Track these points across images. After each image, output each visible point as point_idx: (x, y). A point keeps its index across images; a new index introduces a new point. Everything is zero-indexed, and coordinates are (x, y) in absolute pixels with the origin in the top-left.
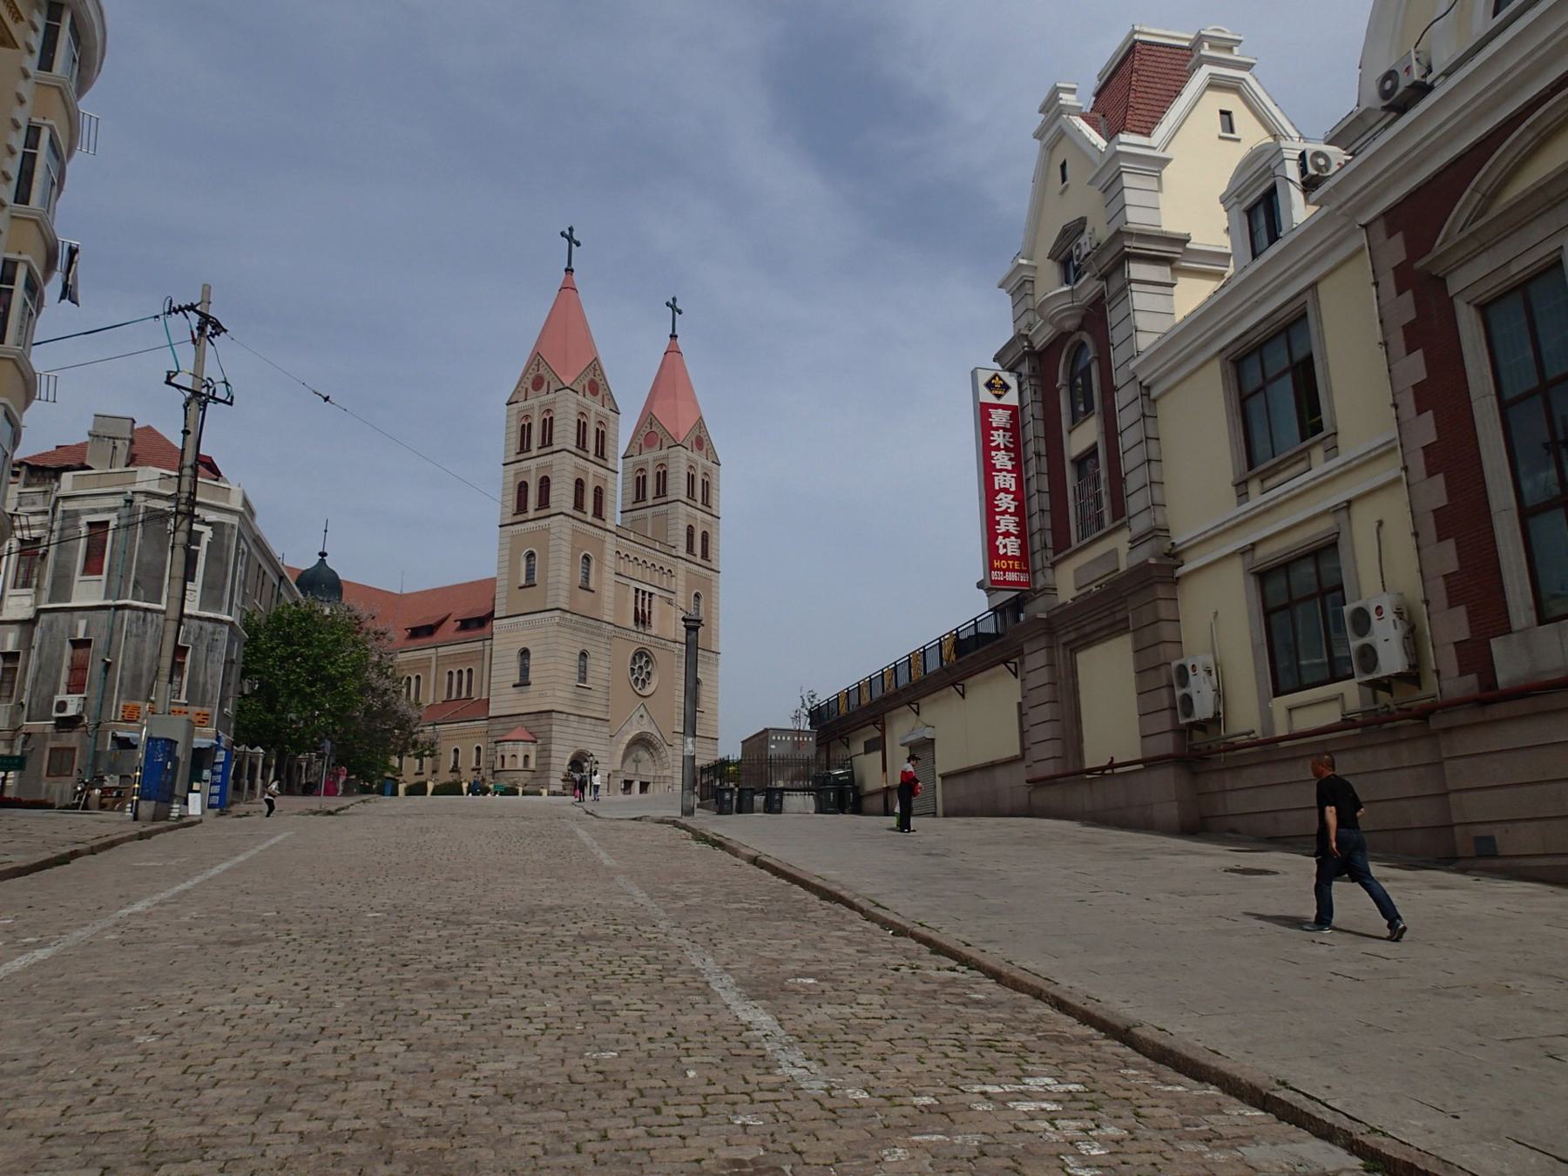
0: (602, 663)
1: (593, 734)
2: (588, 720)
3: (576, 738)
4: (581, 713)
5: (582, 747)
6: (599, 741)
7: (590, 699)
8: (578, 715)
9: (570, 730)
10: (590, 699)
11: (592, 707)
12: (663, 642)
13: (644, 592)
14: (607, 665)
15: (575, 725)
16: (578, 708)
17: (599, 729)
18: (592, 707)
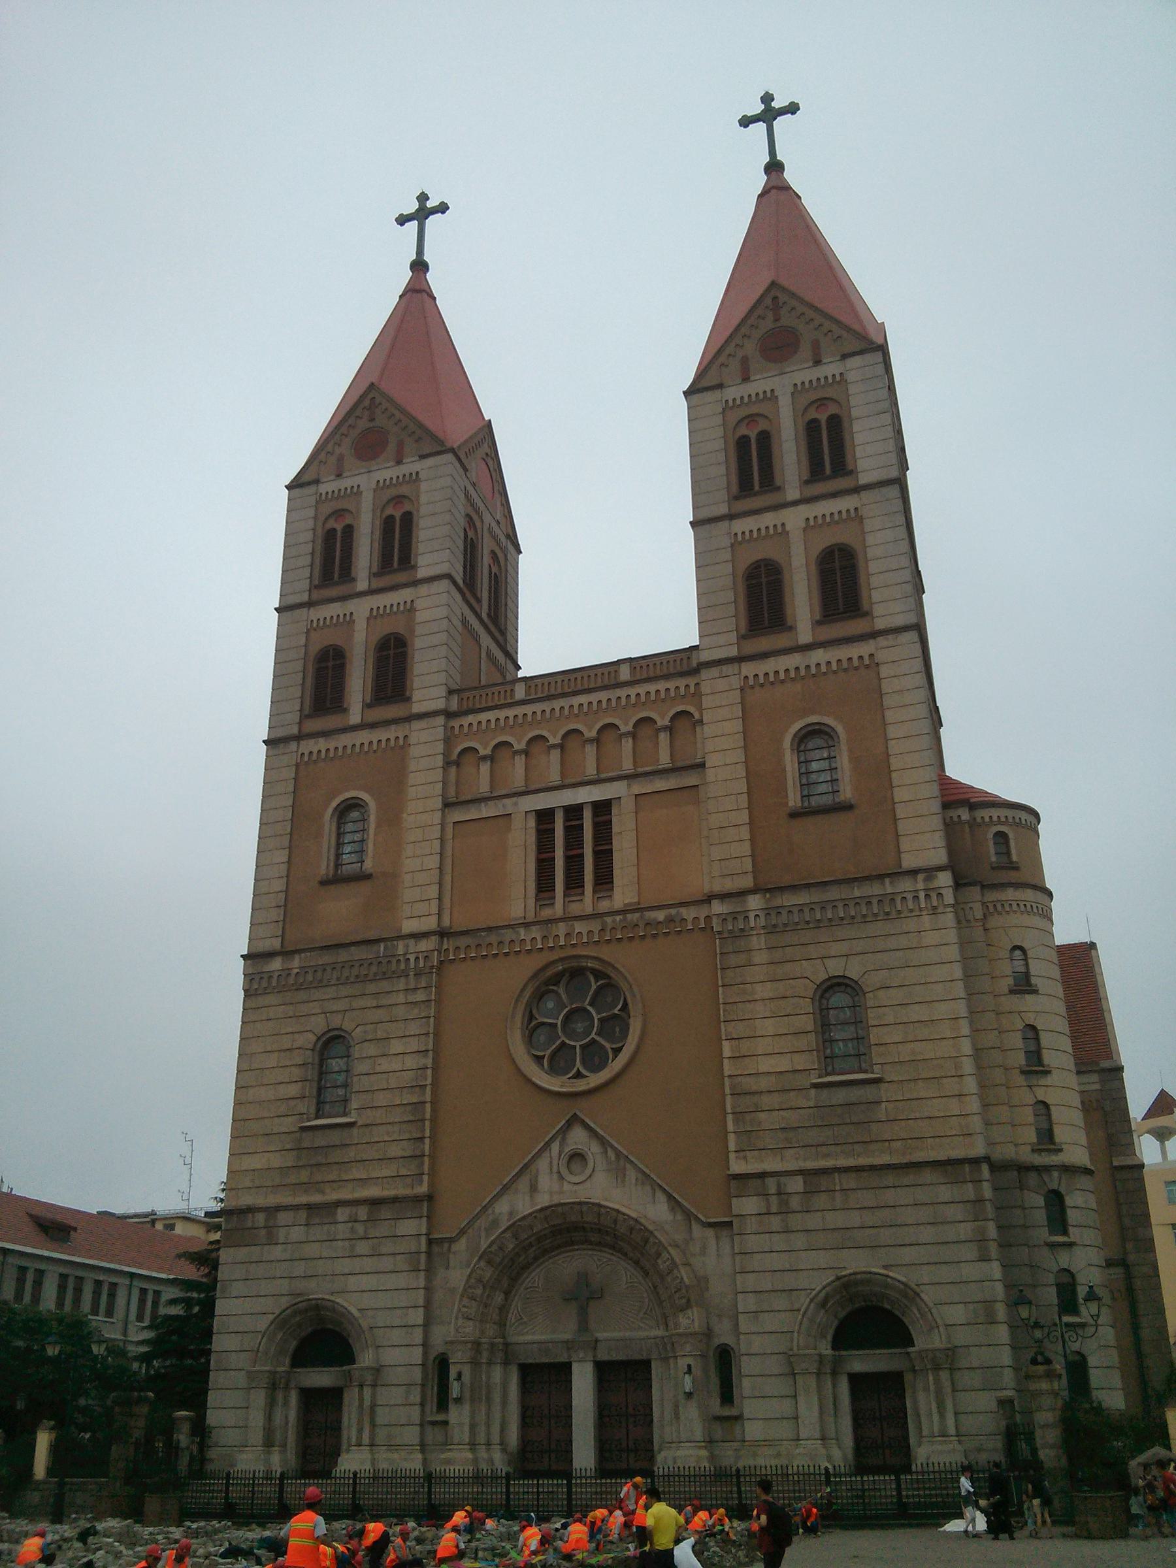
0: (396, 1047)
1: (362, 1247)
2: (342, 1214)
3: (299, 1269)
4: (316, 1198)
5: (317, 1290)
6: (387, 1263)
7: (351, 1154)
8: (310, 1207)
9: (277, 1252)
10: (351, 1154)
11: (357, 1173)
12: (660, 916)
13: (574, 811)
14: (414, 1045)
15: (297, 1233)
16: (306, 1186)
17: (383, 1229)
18: (357, 1173)
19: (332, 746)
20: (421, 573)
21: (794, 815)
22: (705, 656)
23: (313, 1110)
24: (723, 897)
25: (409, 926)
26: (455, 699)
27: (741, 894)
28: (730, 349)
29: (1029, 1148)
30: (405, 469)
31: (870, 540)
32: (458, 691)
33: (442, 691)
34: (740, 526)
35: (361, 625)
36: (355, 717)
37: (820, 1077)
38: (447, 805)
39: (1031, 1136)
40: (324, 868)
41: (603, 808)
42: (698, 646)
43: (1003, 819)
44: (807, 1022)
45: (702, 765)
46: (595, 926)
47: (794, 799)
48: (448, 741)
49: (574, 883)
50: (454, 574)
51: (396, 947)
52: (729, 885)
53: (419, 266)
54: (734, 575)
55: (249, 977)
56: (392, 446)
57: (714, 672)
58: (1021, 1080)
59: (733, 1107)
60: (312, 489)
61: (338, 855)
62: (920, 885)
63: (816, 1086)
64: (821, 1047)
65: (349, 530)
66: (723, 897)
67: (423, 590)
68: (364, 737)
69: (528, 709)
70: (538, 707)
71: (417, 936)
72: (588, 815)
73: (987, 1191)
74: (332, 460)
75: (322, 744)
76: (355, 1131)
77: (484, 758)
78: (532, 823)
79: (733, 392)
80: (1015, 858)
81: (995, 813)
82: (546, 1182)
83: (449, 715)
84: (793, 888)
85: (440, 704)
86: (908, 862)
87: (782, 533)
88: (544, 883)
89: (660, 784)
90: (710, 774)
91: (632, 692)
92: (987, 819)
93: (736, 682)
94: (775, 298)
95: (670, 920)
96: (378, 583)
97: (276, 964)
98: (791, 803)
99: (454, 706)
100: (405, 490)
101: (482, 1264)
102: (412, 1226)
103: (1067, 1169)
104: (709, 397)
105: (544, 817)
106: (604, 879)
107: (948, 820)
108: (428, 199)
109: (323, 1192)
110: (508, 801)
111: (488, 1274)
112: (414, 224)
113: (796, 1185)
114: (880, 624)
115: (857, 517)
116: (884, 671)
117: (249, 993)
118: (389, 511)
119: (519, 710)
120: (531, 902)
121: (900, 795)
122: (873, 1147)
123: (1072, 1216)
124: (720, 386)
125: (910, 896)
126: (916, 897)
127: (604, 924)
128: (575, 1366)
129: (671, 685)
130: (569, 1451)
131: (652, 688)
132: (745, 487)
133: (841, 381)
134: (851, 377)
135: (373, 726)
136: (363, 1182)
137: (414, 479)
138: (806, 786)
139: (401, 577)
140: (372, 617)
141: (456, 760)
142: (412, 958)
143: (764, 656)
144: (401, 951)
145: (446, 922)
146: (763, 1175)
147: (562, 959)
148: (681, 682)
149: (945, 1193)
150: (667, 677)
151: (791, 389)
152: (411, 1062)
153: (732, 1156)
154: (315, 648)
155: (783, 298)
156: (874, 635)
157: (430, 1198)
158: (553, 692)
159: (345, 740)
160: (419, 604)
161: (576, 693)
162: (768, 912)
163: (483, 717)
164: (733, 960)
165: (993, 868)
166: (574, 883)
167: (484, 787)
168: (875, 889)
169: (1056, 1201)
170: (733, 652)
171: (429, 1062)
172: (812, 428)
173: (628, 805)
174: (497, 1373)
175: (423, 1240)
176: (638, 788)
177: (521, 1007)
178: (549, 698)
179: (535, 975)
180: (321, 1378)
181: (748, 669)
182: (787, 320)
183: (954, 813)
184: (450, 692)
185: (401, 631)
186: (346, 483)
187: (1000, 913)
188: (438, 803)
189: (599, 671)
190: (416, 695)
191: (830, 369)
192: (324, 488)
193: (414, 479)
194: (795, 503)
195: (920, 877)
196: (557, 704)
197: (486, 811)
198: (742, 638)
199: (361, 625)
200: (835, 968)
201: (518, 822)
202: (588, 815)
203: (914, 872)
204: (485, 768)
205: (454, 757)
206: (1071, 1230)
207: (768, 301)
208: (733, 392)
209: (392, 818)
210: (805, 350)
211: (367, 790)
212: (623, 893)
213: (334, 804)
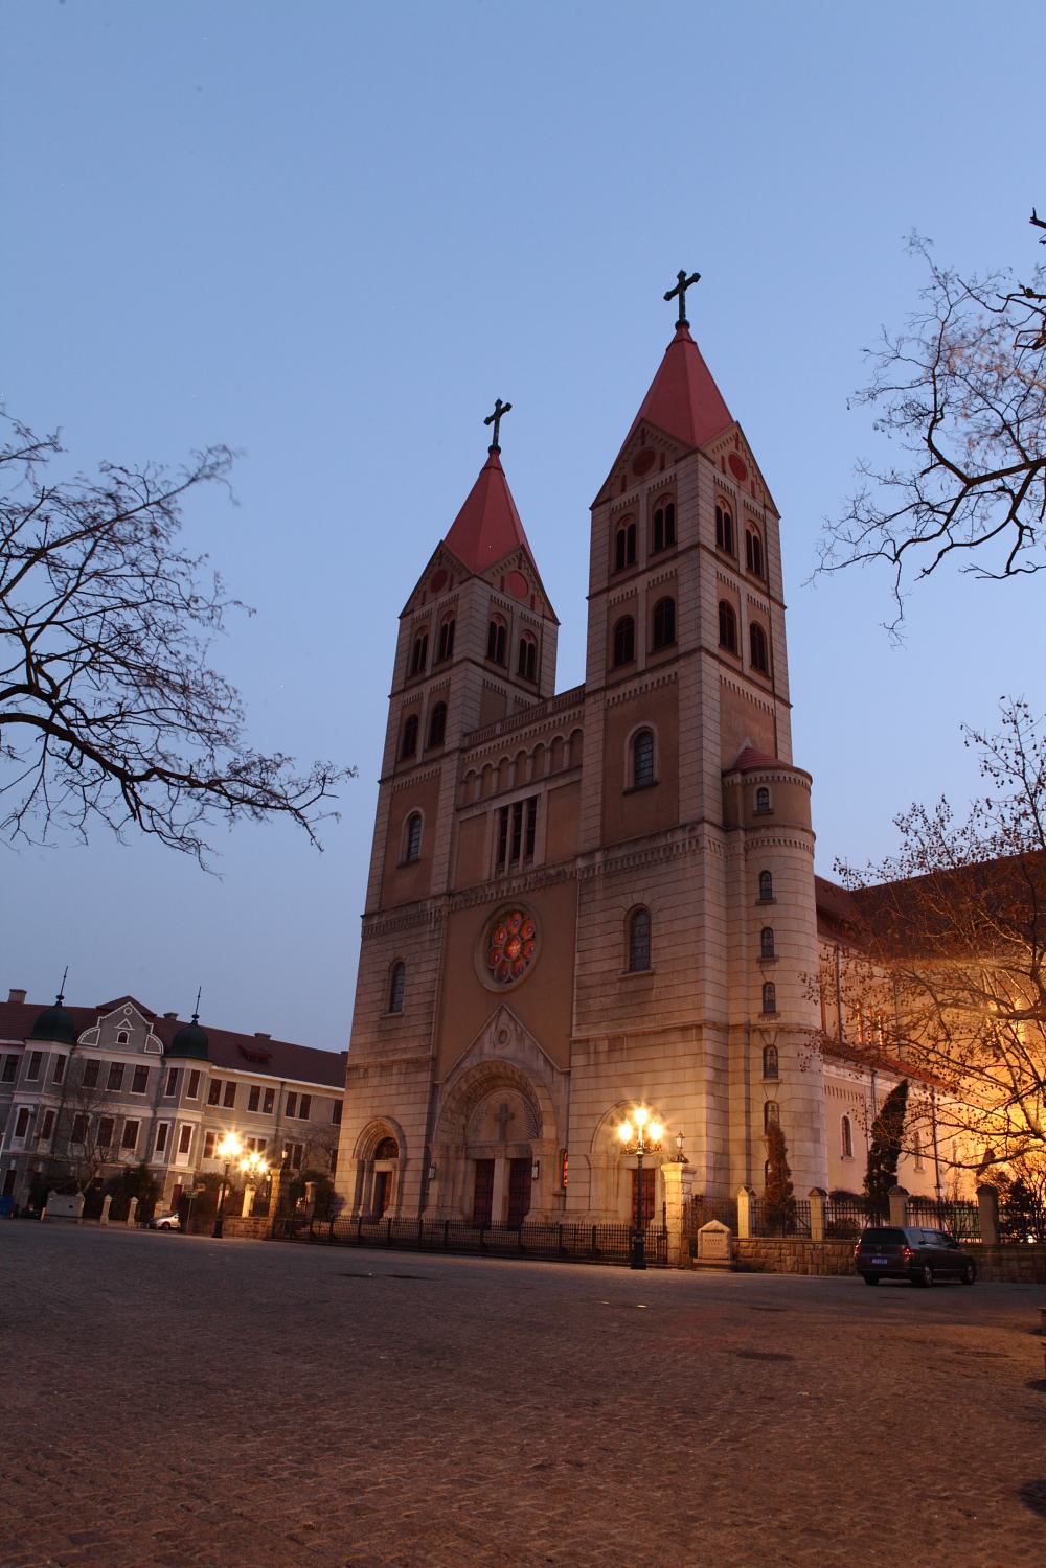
13: (518, 806)
14: (432, 966)
21: (626, 793)
22: (587, 690)
23: (388, 1007)
24: (583, 855)
25: (435, 890)
26: (467, 739)
27: (590, 854)
29: (757, 1015)
31: (682, 590)
32: (469, 734)
34: (614, 594)
35: (425, 700)
37: (624, 973)
38: (458, 810)
39: (759, 1006)
40: (401, 857)
41: (532, 801)
43: (764, 779)
44: (619, 937)
45: (581, 766)
46: (521, 882)
47: (628, 783)
48: (460, 768)
49: (515, 855)
50: (472, 656)
51: (425, 905)
52: (583, 847)
53: (495, 450)
54: (607, 631)
55: (365, 929)
57: (591, 700)
58: (756, 967)
59: (578, 996)
60: (410, 616)
61: (409, 849)
62: (687, 836)
63: (621, 980)
64: (628, 954)
65: (426, 638)
66: (583, 855)
71: (436, 897)
72: (525, 807)
73: (708, 1047)
74: (421, 594)
75: (405, 779)
76: (403, 1020)
77: (477, 777)
78: (497, 817)
80: (770, 806)
81: (759, 774)
82: (487, 1049)
83: (463, 750)
84: (620, 845)
85: (455, 745)
86: (682, 821)
87: (634, 595)
88: (501, 858)
89: (561, 782)
90: (584, 773)
91: (556, 718)
92: (753, 780)
93: (602, 705)
94: (644, 429)
95: (558, 874)
96: (438, 669)
97: (375, 921)
98: (625, 786)
100: (452, 607)
101: (451, 1098)
102: (425, 1076)
103: (782, 1030)
104: (602, 508)
105: (504, 811)
106: (530, 851)
107: (726, 784)
108: (501, 403)
109: (387, 1056)
110: (486, 804)
111: (453, 1105)
113: (603, 1046)
114: (682, 650)
115: (674, 576)
116: (681, 683)
117: (364, 937)
119: (500, 741)
120: (493, 870)
121: (682, 772)
122: (646, 1019)
123: (782, 1063)
125: (680, 844)
126: (684, 845)
127: (526, 880)
128: (496, 1162)
129: (571, 712)
130: (490, 1214)
131: (562, 715)
135: (425, 764)
136: (404, 1050)
137: (456, 599)
138: (637, 771)
141: (464, 781)
142: (433, 910)
143: (618, 684)
144: (428, 907)
145: (452, 887)
146: (587, 1041)
147: (504, 906)
148: (577, 710)
149: (680, 1048)
150: (570, 707)
151: (647, 492)
152: (430, 976)
153: (574, 1028)
154: (406, 717)
156: (677, 658)
157: (435, 1059)
161: (523, 726)
162: (605, 863)
163: (479, 749)
164: (585, 898)
165: (755, 816)
166: (515, 855)
168: (662, 842)
169: (770, 1052)
170: (602, 683)
171: (437, 976)
172: (658, 516)
173: (544, 798)
174: (462, 1163)
175: (428, 1084)
176: (551, 786)
177: (483, 938)
178: (510, 731)
179: (490, 917)
180: (382, 1166)
181: (610, 695)
183: (728, 779)
184: (465, 735)
185: (443, 700)
187: (755, 849)
188: (451, 810)
190: (447, 740)
192: (417, 614)
194: (644, 572)
195: (688, 828)
196: (514, 735)
197: (476, 812)
198: (608, 673)
199: (425, 700)
200: (637, 898)
201: (490, 817)
202: (525, 807)
203: (684, 826)
205: (464, 778)
206: (780, 1072)
207: (639, 433)
209: (432, 823)
211: (418, 806)
212: (538, 858)
213: (407, 816)
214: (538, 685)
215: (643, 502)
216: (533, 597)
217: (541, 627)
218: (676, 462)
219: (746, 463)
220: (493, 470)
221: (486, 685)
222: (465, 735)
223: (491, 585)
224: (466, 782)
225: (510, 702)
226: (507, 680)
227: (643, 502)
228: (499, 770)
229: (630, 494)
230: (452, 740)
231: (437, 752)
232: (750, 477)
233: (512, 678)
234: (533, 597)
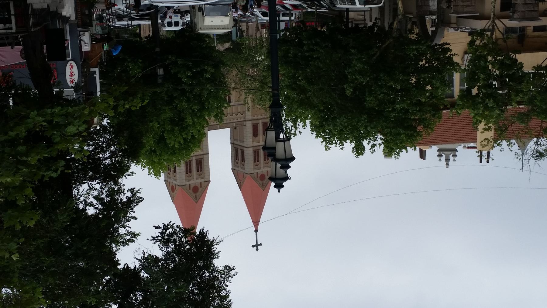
19: (264, 116)
20: (251, 149)
26: (245, 124)
28: (203, 189)
30: (256, 171)
33: (247, 125)
36: (260, 121)
42: (208, 131)
53: (256, 231)
56: (259, 176)
67: (252, 145)
68: (259, 117)
69: (233, 121)
70: (231, 121)
78: (231, 100)
79: (202, 180)
83: (245, 121)
85: (247, 122)
94: (196, 200)
99: (245, 122)
100: (256, 167)
112: (259, 243)
118: (258, 163)
124: (205, 182)
132: (201, 161)
133: (186, 180)
134: (185, 181)
135: (257, 119)
137: (255, 169)
139: (255, 148)
140: (259, 141)
150: (212, 125)
155: (195, 200)
158: (229, 124)
159: (261, 117)
160: (252, 143)
163: (240, 120)
167: (239, 107)
178: (230, 123)
182: (194, 195)
185: (254, 138)
186: (266, 169)
189: (222, 128)
191: (188, 183)
193: (255, 169)
196: (229, 122)
201: (234, 102)
204: (239, 111)
205: (244, 113)
207: (197, 199)
208: (202, 180)
210: (192, 187)
214: (234, 147)
215: (195, 177)
216: (237, 175)
217: (235, 166)
218: (186, 185)
219: (171, 192)
220: (256, 223)
221: (243, 142)
222: (245, 125)
223: (246, 173)
224: (243, 112)
225: (239, 140)
226: (240, 145)
227: (195, 177)
228: (233, 113)
229: (198, 181)
230: (249, 125)
231: (255, 122)
232: (170, 188)
233: (239, 147)
234: (237, 175)
